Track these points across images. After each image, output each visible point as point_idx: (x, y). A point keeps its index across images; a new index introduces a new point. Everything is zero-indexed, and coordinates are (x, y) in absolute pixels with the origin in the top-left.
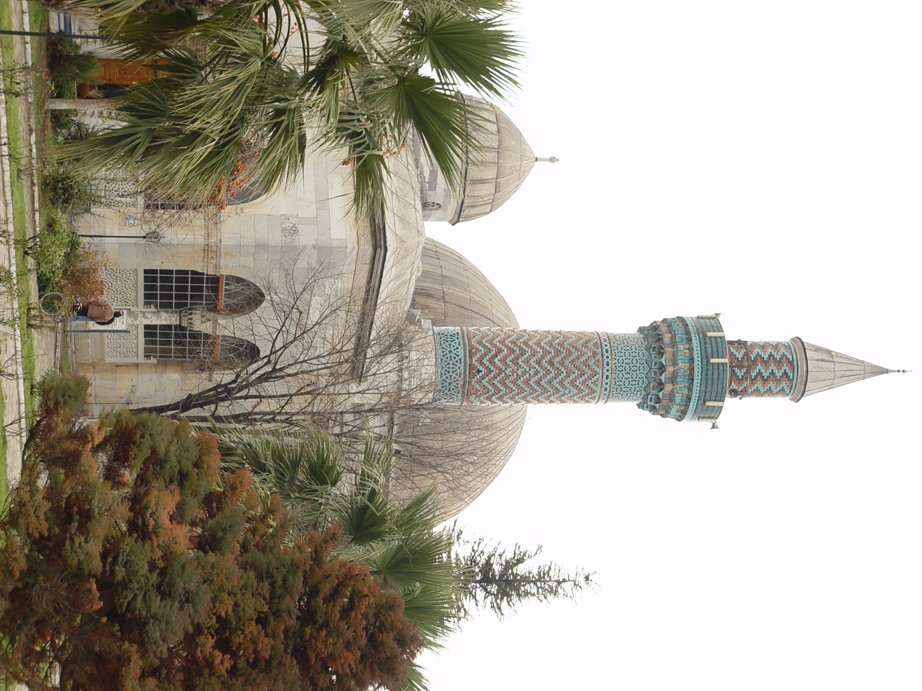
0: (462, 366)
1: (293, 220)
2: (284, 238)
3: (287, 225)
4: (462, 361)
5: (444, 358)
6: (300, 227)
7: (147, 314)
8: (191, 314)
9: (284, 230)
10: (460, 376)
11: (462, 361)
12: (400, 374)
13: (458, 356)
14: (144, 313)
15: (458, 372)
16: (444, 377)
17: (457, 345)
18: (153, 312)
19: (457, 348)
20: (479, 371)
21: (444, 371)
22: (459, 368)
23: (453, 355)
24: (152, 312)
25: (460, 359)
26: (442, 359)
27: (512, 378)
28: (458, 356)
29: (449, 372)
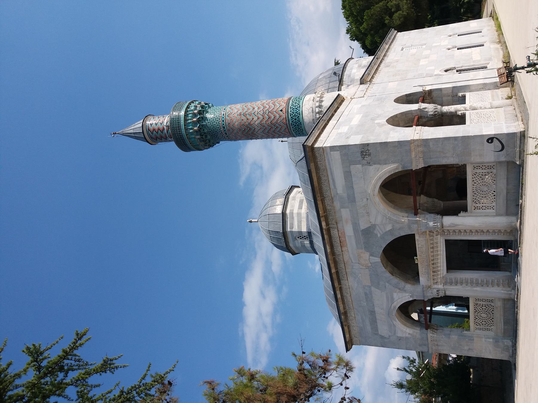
0: (290, 112)
1: (365, 162)
2: (369, 149)
3: (367, 158)
4: (289, 115)
5: (298, 115)
6: (360, 158)
7: (464, 109)
8: (435, 112)
9: (369, 155)
10: (291, 107)
11: (289, 115)
13: (292, 118)
14: (466, 110)
15: (291, 109)
16: (298, 106)
17: (293, 123)
18: (459, 111)
19: (292, 122)
20: (281, 111)
21: (298, 109)
22: (291, 111)
23: (296, 117)
24: (461, 111)
25: (291, 116)
26: (299, 115)
27: (266, 109)
28: (292, 118)
29: (296, 109)
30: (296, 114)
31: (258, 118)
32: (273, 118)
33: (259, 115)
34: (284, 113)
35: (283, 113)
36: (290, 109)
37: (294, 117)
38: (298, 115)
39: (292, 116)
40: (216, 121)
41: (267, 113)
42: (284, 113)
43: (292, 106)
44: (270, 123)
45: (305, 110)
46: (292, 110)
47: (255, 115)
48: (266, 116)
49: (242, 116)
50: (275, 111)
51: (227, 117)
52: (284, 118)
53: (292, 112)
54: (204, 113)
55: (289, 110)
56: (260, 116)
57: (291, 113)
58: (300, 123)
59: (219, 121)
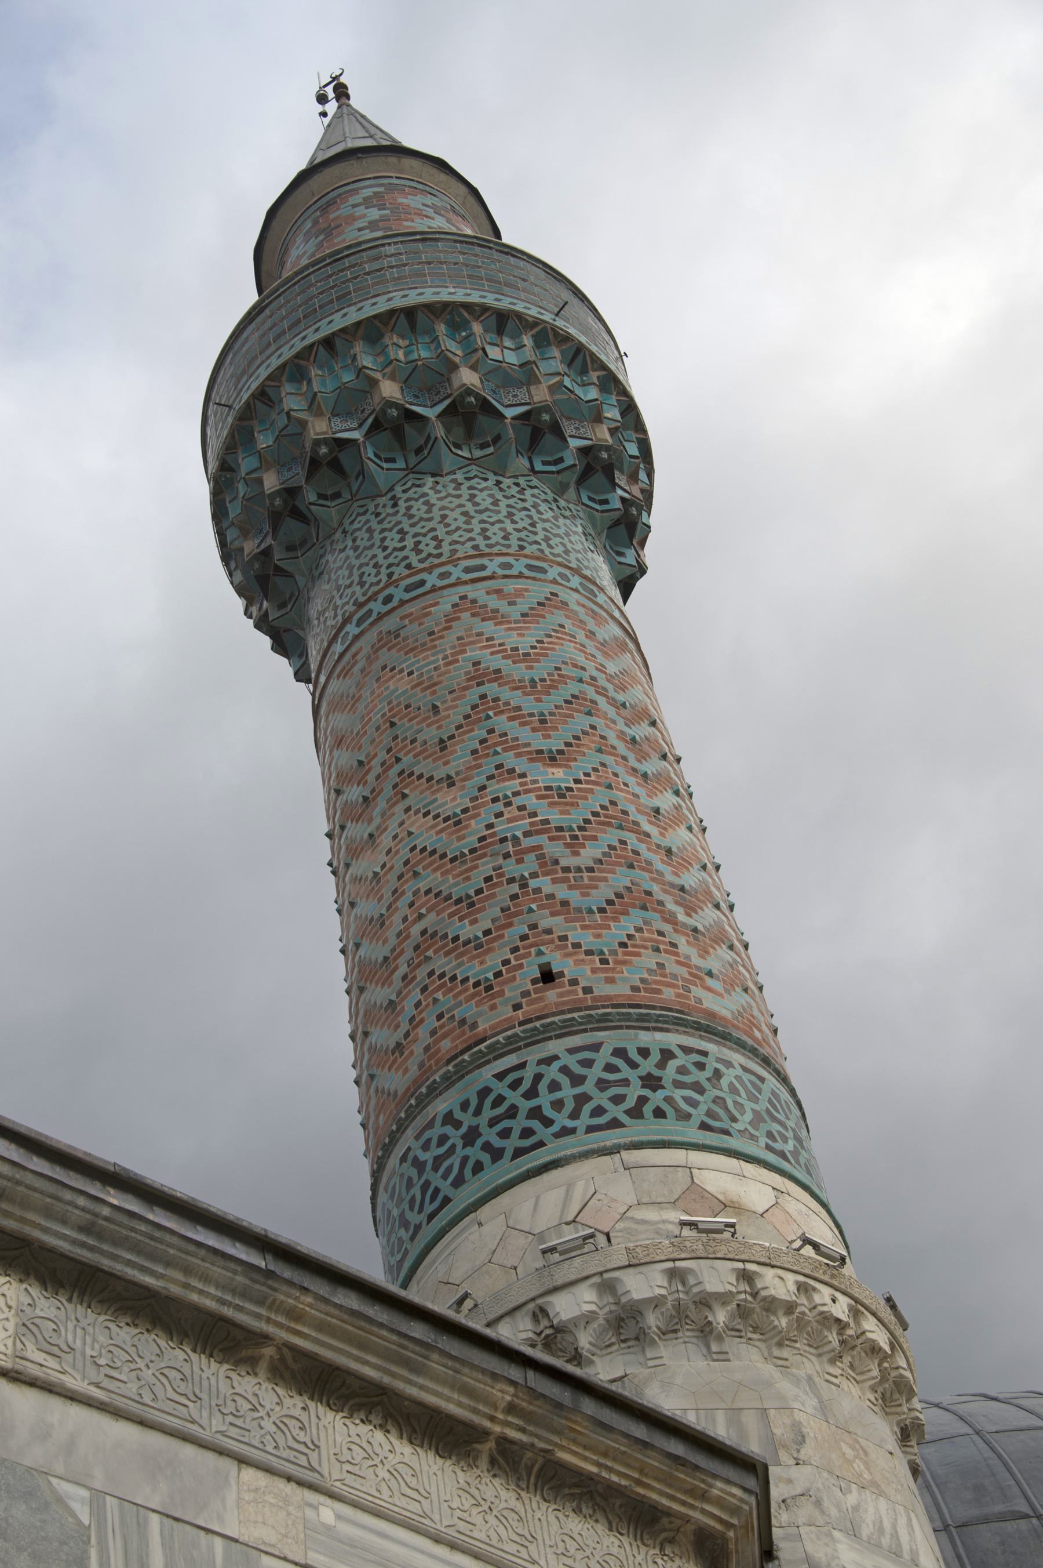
4: (511, 1060)
10: (596, 1047)
12: (652, 1320)
15: (571, 1061)
20: (548, 976)
21: (585, 1119)
26: (519, 1153)
27: (554, 849)
30: (522, 1114)
31: (456, 821)
32: (467, 930)
33: (486, 815)
34: (517, 1007)
35: (525, 994)
36: (571, 1051)
37: (488, 1113)
38: (514, 1142)
39: (501, 1088)
40: (409, 542)
41: (511, 868)
42: (517, 1007)
43: (604, 1055)
44: (424, 932)
45: (570, 1187)
46: (565, 1070)
47: (483, 788)
48: (486, 867)
49: (473, 695)
50: (533, 926)
51: (452, 596)
52: (474, 1025)
53: (538, 1078)
54: (483, 446)
55: (555, 1047)
56: (476, 827)
57: (528, 1074)
58: (447, 1200)
59: (414, 560)
